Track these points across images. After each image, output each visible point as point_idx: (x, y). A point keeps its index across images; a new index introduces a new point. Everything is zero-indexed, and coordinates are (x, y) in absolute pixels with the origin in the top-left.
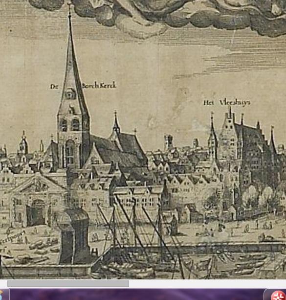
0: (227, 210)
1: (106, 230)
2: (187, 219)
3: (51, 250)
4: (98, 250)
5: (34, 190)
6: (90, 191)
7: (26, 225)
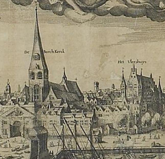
0: (132, 127)
1: (58, 140)
2: (107, 133)
3: (25, 152)
4: (54, 152)
5: (14, 115)
6: (49, 116)
7: (10, 136)
